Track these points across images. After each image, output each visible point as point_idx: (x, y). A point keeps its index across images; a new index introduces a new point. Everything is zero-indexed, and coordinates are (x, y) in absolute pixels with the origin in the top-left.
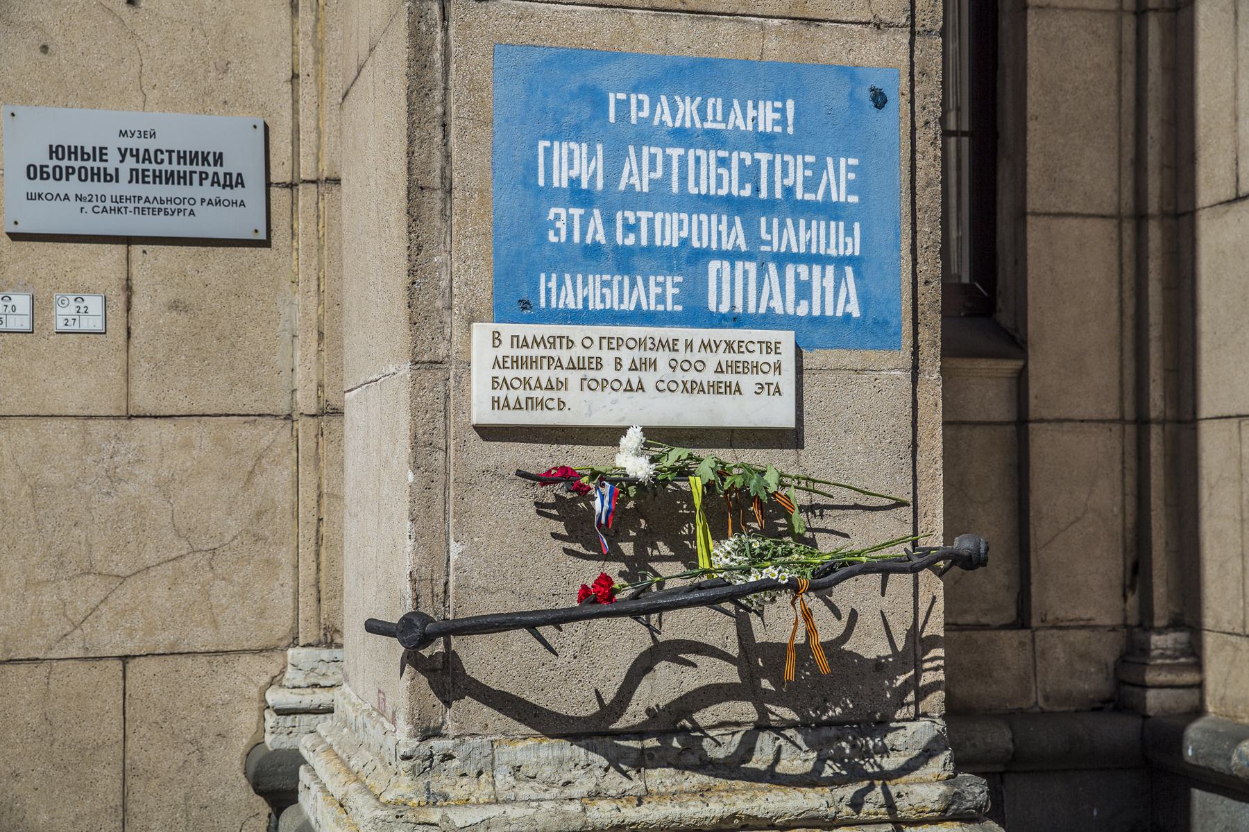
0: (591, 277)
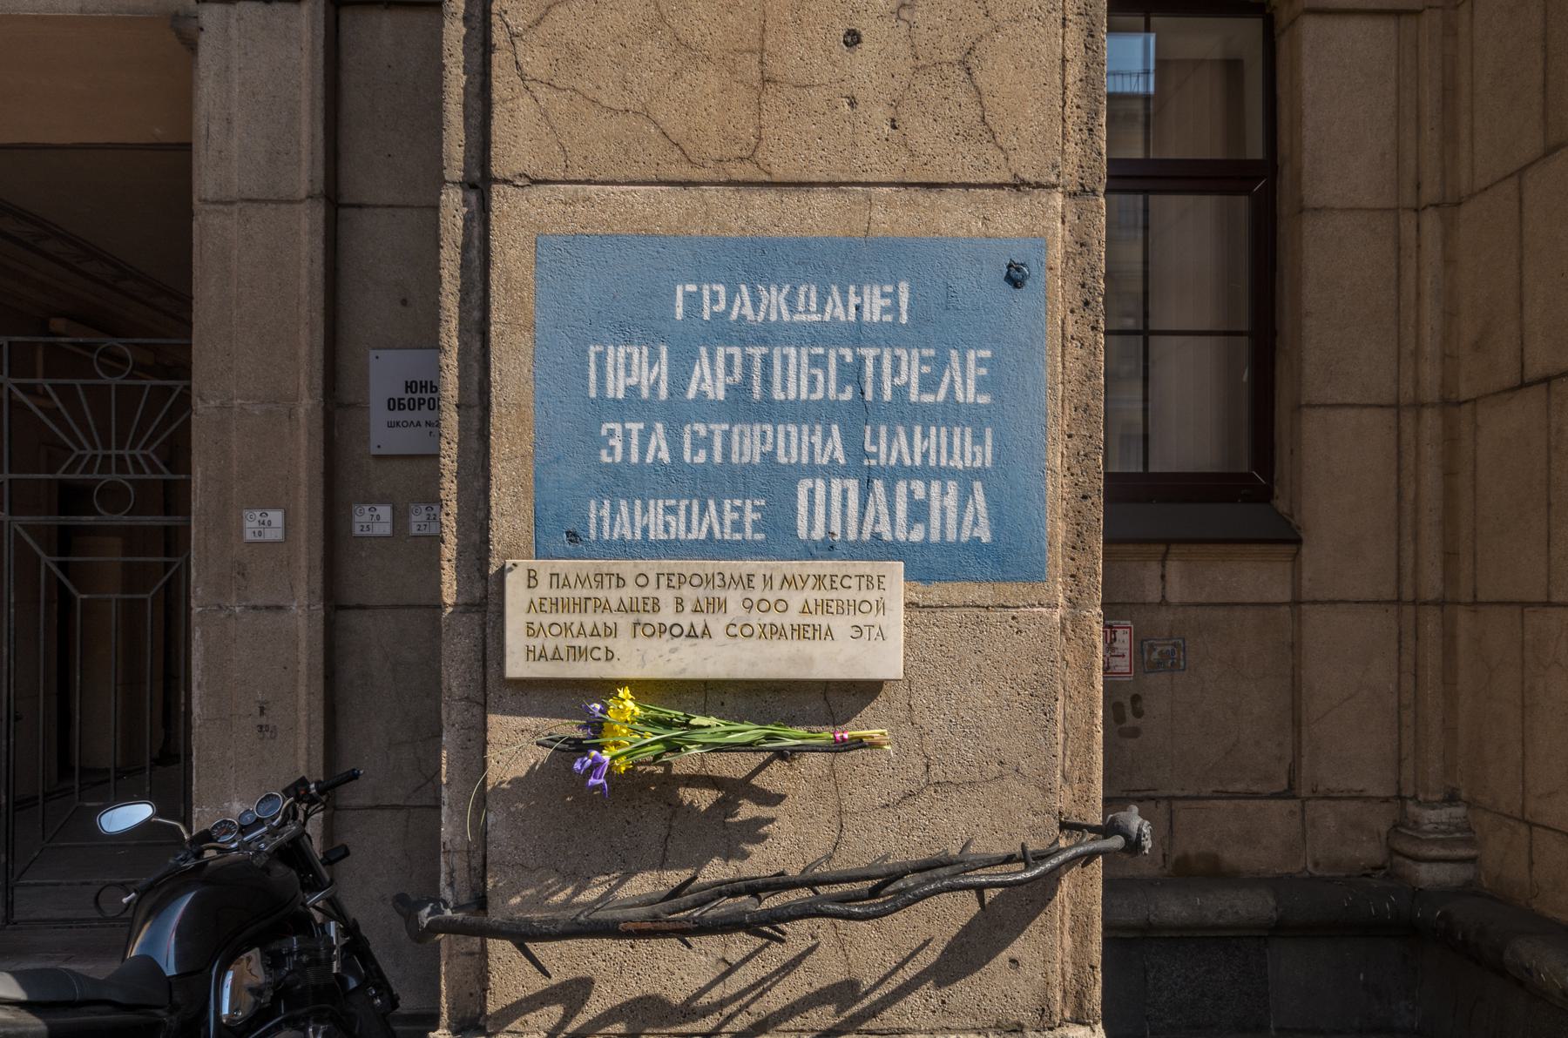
0: (652, 502)
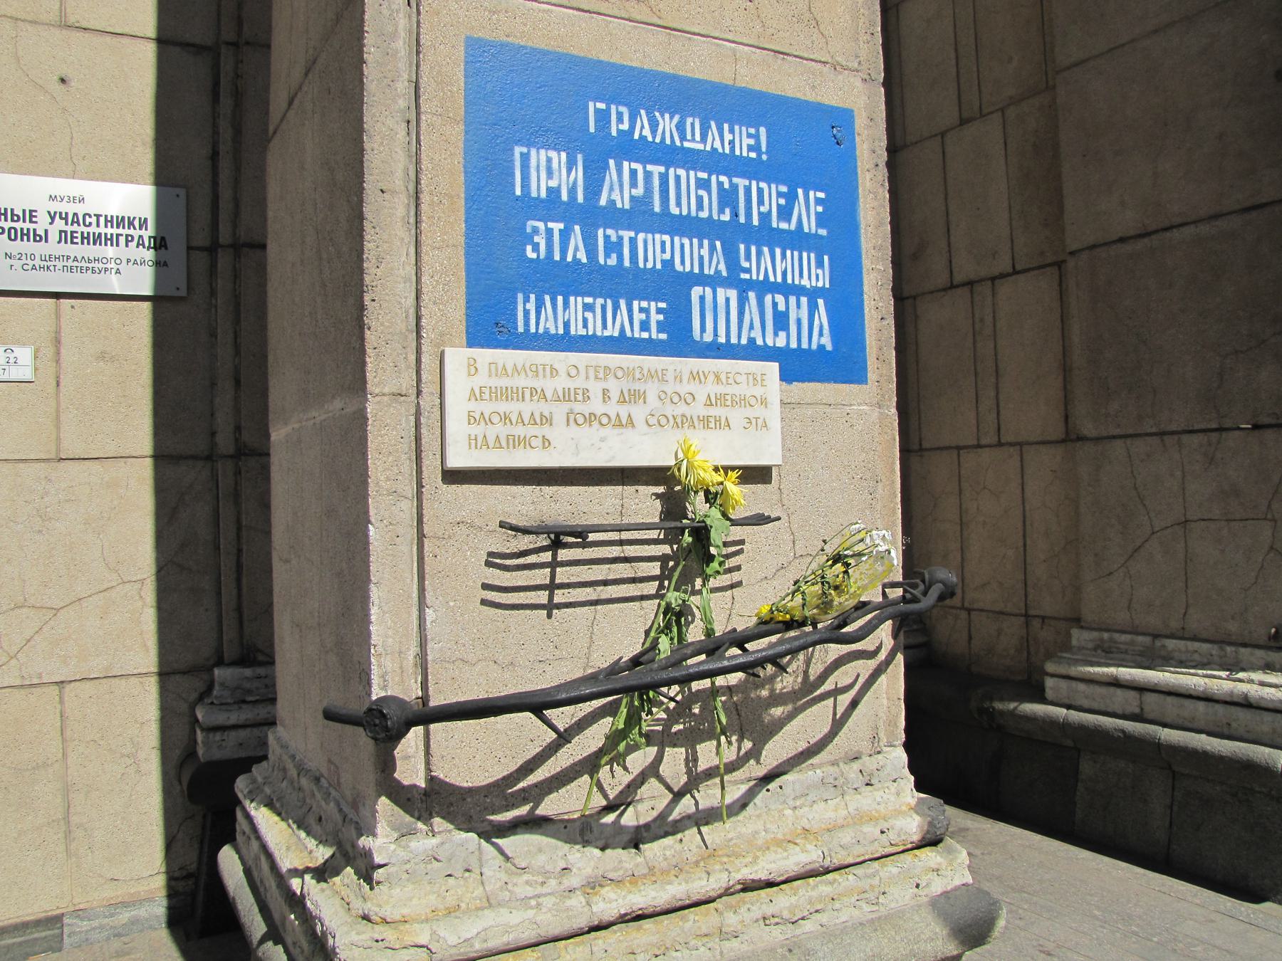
0: (572, 299)
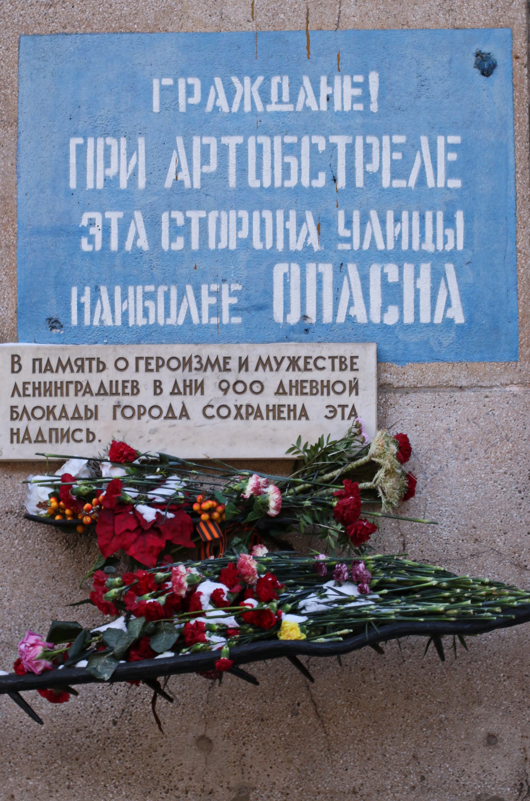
0: (131, 289)
